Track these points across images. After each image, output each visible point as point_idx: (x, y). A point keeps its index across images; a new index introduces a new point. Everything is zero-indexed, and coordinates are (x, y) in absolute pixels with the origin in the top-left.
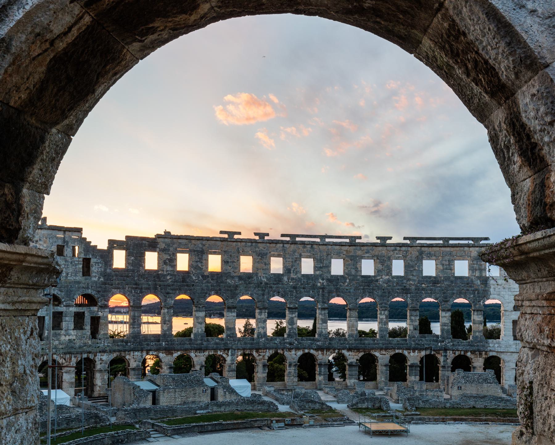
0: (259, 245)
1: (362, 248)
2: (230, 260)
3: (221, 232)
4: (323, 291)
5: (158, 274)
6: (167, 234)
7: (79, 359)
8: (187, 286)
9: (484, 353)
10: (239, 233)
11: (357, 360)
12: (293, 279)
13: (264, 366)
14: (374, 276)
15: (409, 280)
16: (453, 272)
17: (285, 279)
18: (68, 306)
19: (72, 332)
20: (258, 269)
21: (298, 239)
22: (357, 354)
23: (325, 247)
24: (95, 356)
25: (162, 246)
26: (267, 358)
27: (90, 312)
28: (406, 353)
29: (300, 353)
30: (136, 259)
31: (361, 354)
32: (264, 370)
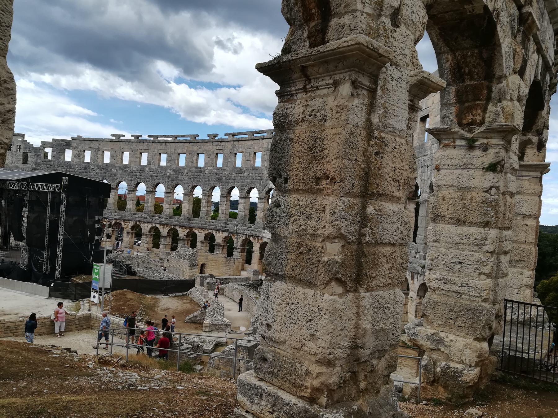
1: (198, 144)
2: (114, 155)
4: (168, 179)
8: (86, 172)
9: (260, 238)
11: (184, 235)
12: (152, 169)
13: (128, 233)
15: (224, 170)
16: (252, 162)
17: (147, 169)
21: (159, 139)
22: (184, 230)
25: (74, 145)
26: (130, 227)
28: (214, 233)
29: (150, 226)
31: (188, 231)
32: (128, 236)
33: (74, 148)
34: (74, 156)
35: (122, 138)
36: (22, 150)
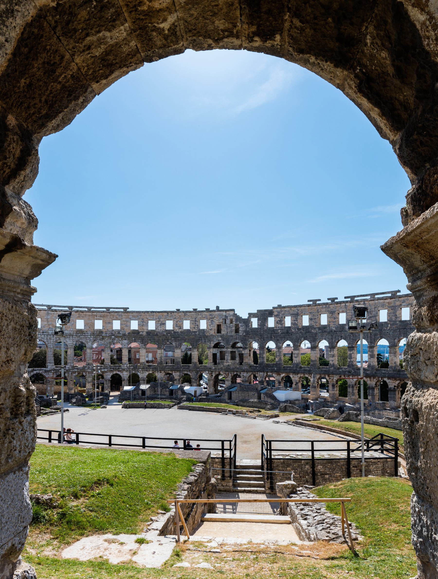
0: (331, 306)
1: (400, 299)
3: (309, 301)
5: (274, 330)
6: (280, 306)
7: (233, 375)
10: (320, 300)
14: (409, 321)
18: (227, 348)
19: (229, 361)
20: (330, 322)
23: (373, 302)
24: (240, 373)
25: (276, 313)
27: (238, 351)
30: (262, 322)
33: (276, 316)
34: (277, 322)
35: (318, 302)
36: (234, 323)
